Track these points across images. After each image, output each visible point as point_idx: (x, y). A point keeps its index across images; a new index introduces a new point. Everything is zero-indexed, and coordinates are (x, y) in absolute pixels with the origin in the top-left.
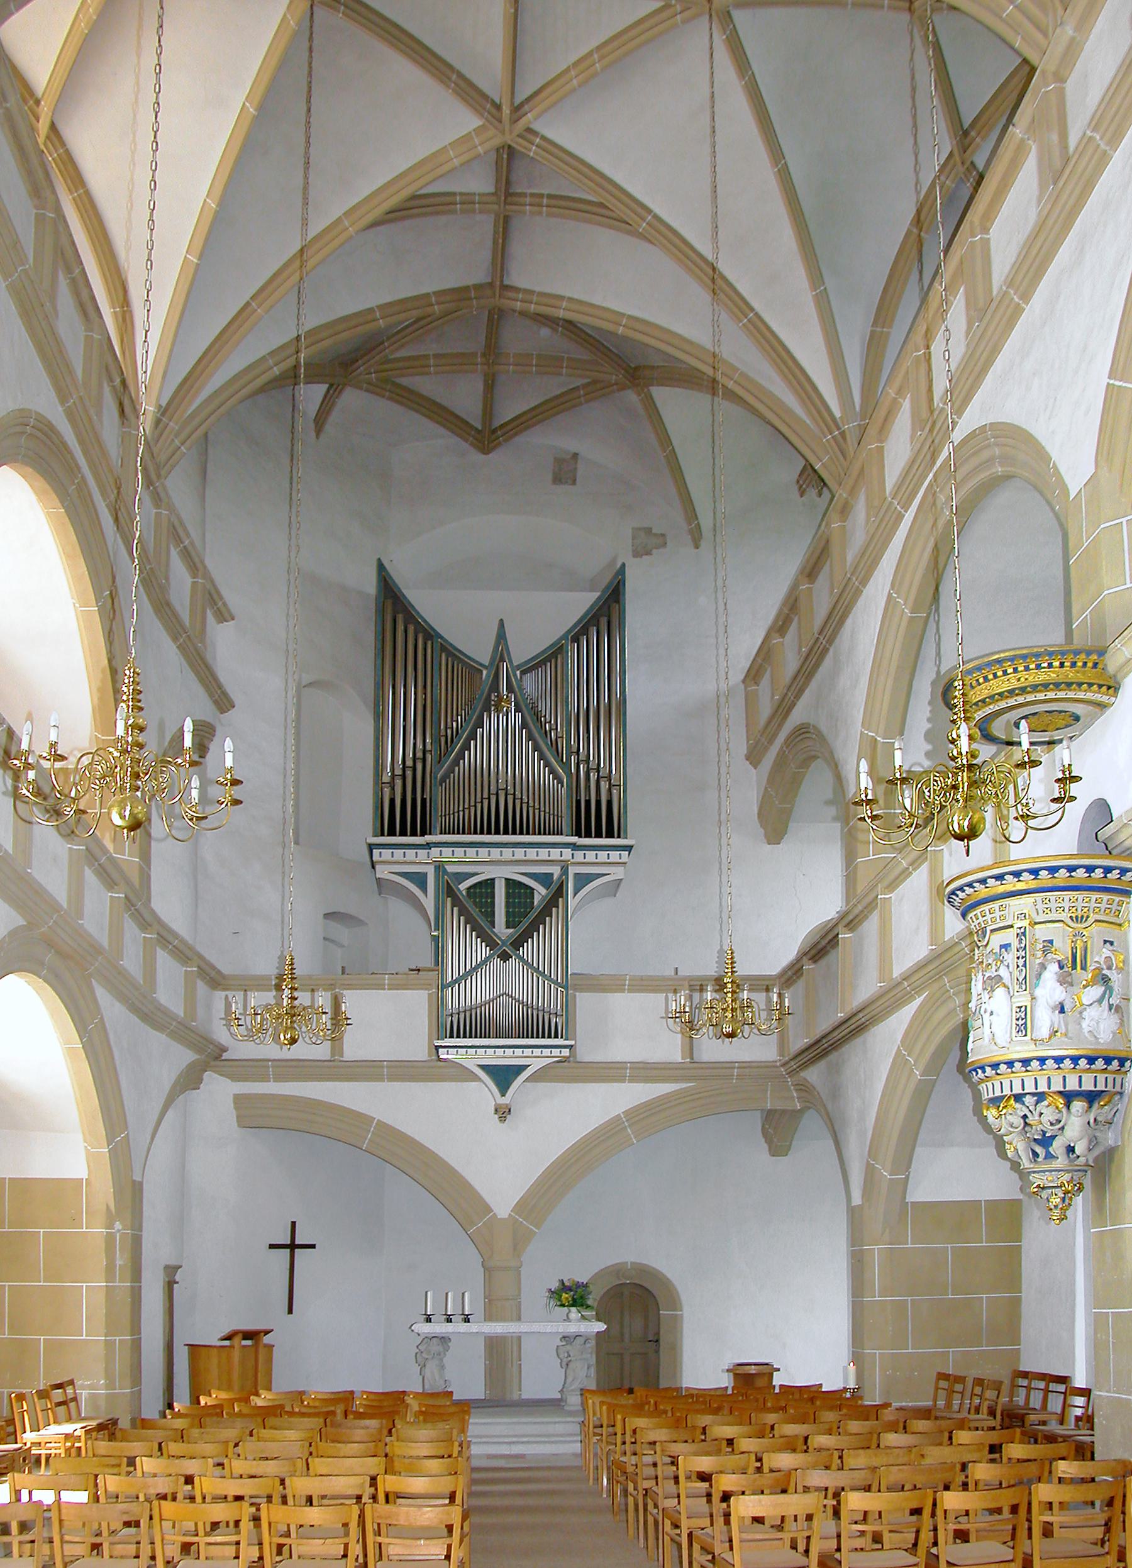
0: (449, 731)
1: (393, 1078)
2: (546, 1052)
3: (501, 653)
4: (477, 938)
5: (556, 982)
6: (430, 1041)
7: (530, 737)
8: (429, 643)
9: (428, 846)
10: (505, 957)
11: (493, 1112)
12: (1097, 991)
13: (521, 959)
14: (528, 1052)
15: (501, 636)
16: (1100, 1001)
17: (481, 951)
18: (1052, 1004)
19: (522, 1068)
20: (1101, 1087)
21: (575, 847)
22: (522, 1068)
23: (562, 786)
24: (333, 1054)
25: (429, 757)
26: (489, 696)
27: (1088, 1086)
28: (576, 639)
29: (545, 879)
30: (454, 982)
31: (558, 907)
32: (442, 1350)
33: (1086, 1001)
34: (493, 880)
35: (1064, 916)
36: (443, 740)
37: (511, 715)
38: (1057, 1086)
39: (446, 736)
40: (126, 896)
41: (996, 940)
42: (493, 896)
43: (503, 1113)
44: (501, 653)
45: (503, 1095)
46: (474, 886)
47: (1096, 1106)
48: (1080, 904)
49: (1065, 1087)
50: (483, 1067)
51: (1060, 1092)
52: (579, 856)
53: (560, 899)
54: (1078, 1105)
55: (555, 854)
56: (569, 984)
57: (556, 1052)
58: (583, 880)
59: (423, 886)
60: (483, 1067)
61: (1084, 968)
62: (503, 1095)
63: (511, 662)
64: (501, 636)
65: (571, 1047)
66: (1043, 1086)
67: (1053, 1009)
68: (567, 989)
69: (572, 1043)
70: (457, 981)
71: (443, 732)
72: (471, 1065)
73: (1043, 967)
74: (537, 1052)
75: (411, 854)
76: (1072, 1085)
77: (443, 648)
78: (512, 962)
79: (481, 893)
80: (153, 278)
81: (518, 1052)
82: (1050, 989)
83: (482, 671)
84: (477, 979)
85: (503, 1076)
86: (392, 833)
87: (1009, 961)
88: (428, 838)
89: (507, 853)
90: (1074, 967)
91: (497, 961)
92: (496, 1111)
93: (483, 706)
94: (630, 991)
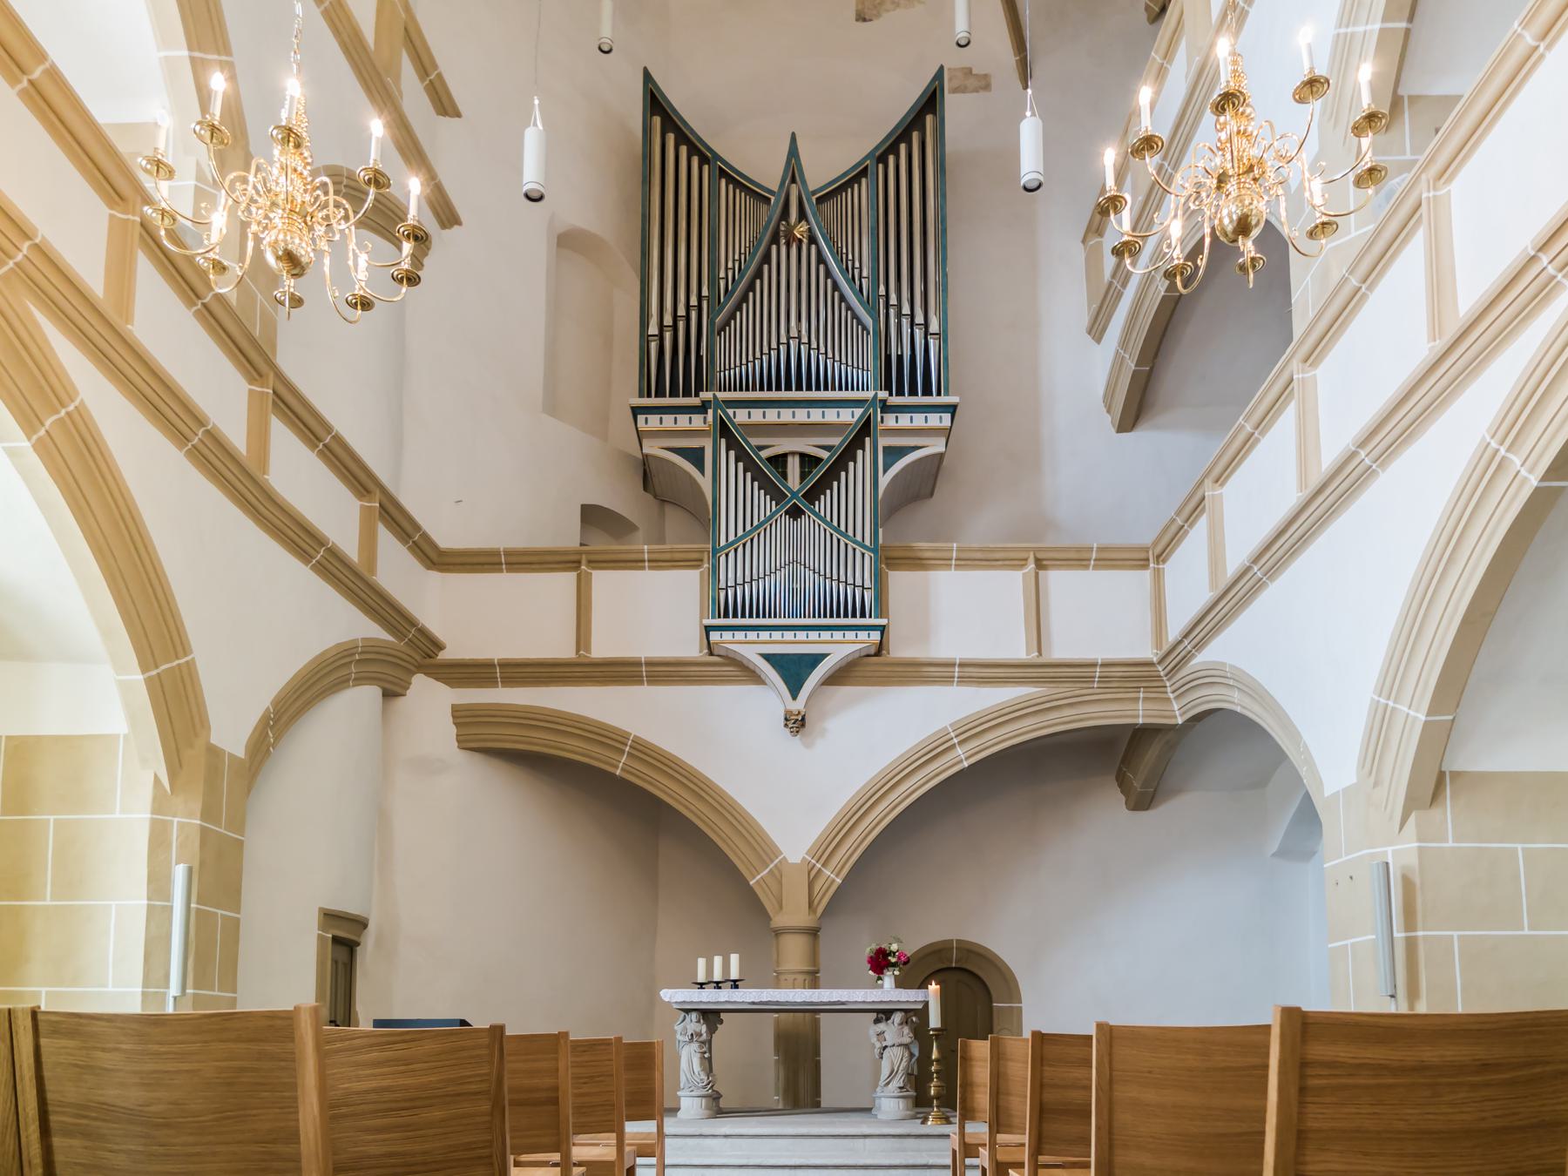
1: (655, 679)
2: (850, 635)
3: (793, 172)
4: (753, 480)
6: (701, 622)
11: (782, 722)
13: (817, 515)
14: (826, 635)
17: (764, 505)
19: (817, 659)
22: (816, 659)
25: (705, 304)
28: (882, 159)
32: (704, 1028)
34: (785, 456)
40: (275, 392)
44: (793, 172)
45: (794, 697)
50: (768, 657)
57: (863, 635)
60: (768, 657)
62: (794, 697)
63: (804, 182)
65: (883, 629)
68: (874, 550)
69: (883, 622)
71: (722, 275)
74: (838, 635)
75: (683, 421)
81: (813, 635)
85: (794, 670)
92: (786, 719)
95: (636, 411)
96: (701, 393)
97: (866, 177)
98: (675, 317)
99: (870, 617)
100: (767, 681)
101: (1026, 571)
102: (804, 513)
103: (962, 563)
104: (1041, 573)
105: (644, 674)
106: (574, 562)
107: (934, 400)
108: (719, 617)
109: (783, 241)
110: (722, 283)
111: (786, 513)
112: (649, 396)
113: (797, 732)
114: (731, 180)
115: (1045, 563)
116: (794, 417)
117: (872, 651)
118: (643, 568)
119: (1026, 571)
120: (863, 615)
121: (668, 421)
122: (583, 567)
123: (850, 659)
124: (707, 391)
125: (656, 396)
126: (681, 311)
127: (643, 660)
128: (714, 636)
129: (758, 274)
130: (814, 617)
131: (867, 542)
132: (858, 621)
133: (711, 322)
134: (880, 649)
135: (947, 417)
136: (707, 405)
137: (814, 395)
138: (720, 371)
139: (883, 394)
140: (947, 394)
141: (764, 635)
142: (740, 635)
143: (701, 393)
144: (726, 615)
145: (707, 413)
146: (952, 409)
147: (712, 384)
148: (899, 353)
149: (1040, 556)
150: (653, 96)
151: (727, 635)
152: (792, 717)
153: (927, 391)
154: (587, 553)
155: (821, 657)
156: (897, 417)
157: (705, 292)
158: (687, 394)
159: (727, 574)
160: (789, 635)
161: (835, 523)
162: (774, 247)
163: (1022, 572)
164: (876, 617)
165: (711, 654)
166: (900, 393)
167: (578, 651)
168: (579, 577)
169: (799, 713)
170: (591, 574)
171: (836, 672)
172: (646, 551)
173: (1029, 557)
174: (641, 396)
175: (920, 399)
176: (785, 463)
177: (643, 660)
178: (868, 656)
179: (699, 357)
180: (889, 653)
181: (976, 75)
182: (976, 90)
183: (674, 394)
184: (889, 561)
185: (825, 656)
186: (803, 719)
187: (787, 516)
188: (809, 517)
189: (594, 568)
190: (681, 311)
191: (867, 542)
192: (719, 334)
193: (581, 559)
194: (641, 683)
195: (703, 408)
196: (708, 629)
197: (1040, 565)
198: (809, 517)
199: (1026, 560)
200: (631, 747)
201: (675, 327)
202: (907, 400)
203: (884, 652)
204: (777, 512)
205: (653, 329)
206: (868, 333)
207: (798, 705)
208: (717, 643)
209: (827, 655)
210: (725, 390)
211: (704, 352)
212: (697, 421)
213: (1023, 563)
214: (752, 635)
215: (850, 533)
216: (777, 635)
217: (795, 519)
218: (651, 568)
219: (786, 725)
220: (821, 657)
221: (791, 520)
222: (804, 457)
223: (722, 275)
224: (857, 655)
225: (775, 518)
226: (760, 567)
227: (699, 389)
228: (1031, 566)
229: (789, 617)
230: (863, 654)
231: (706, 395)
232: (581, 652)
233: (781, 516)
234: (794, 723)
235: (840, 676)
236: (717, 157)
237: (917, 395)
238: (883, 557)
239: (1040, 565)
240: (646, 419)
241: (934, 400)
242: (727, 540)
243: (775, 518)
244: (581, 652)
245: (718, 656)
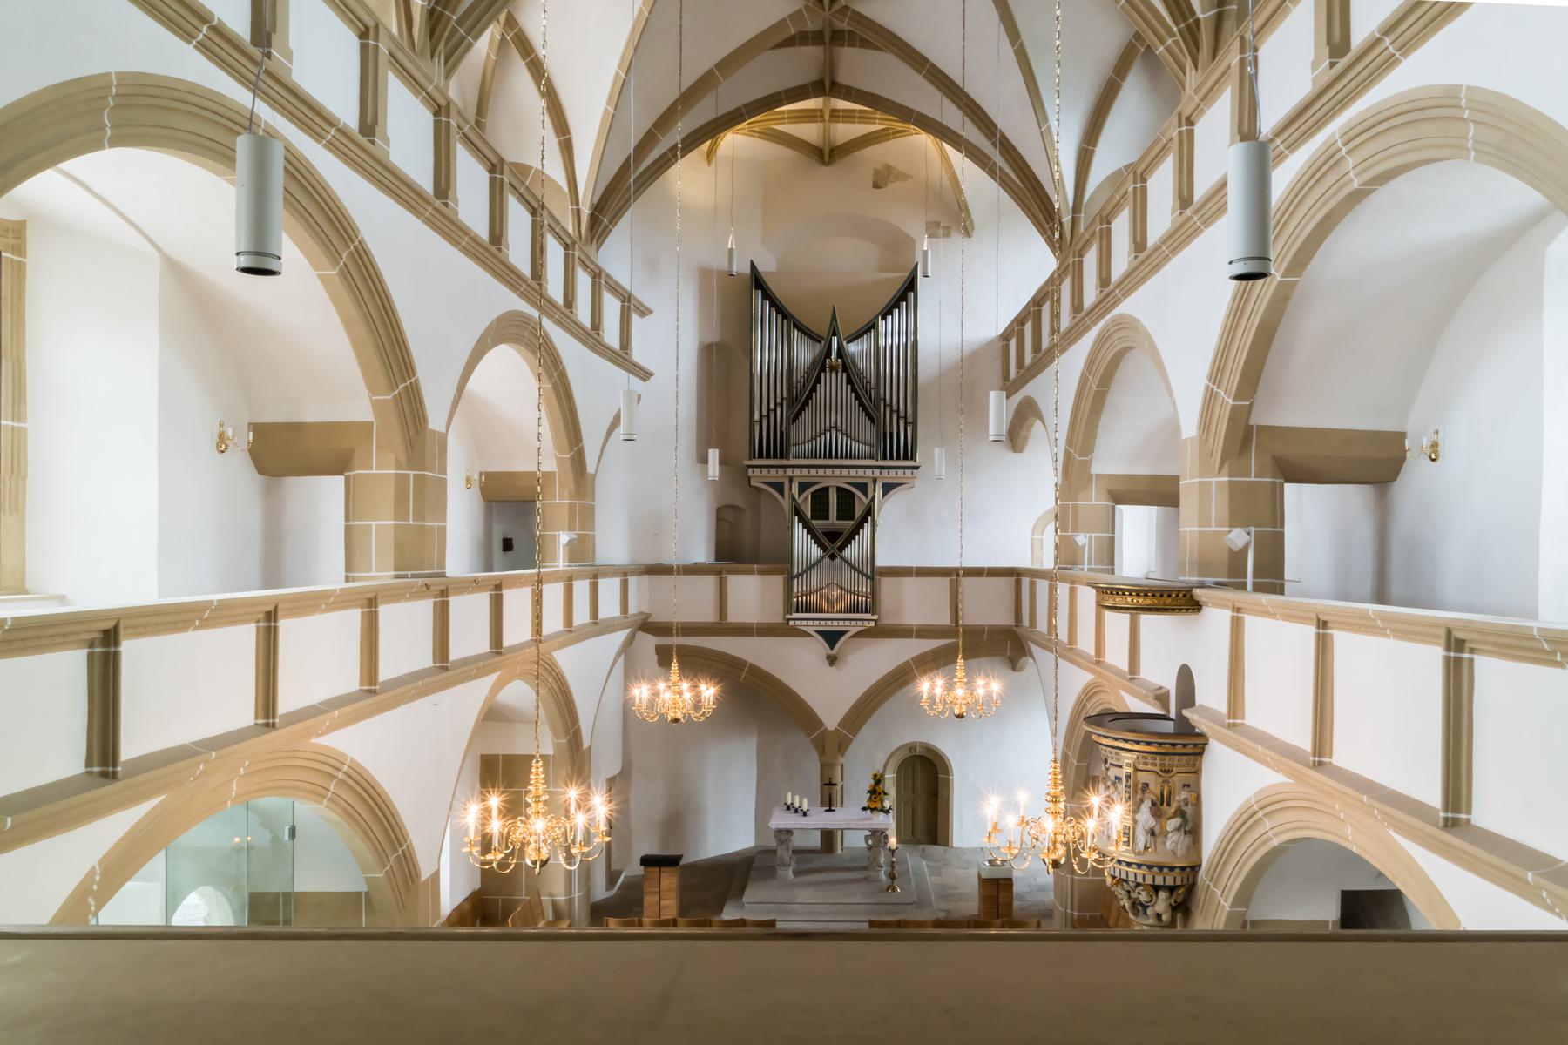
0: (799, 385)
2: (860, 623)
5: (867, 577)
7: (854, 390)
8: (785, 321)
10: (833, 557)
12: (1176, 822)
14: (847, 623)
15: (834, 318)
16: (1178, 829)
18: (1147, 828)
19: (843, 633)
20: (1179, 882)
24: (721, 618)
27: (1170, 882)
28: (884, 318)
29: (863, 488)
33: (1169, 829)
35: (1157, 769)
38: (1149, 881)
39: (797, 388)
41: (1113, 772)
42: (827, 497)
43: (832, 660)
46: (817, 491)
47: (1175, 893)
48: (1167, 762)
49: (1154, 882)
50: (818, 632)
51: (1151, 885)
52: (885, 472)
54: (1162, 895)
55: (869, 472)
56: (875, 574)
57: (866, 623)
58: (888, 488)
59: (782, 493)
60: (818, 632)
61: (1169, 804)
62: (832, 648)
64: (834, 318)
65: (875, 621)
66: (1140, 880)
67: (1147, 832)
69: (875, 617)
71: (794, 386)
72: (810, 630)
73: (1142, 801)
74: (854, 623)
76: (1159, 881)
78: (838, 560)
80: (448, 811)
82: (1145, 817)
84: (814, 572)
85: (831, 638)
86: (761, 456)
87: (1120, 790)
88: (785, 462)
90: (1162, 804)
91: (827, 560)
93: (820, 369)
97: (874, 328)
98: (769, 410)
110: (795, 390)
114: (799, 329)
129: (814, 389)
131: (869, 573)
133: (788, 418)
141: (817, 623)
142: (804, 623)
146: (917, 468)
150: (756, 276)
159: (798, 586)
162: (823, 374)
163: (949, 579)
174: (750, 459)
179: (781, 433)
190: (772, 406)
191: (869, 573)
201: (768, 416)
205: (757, 417)
211: (784, 429)
214: (810, 623)
223: (794, 386)
226: (815, 586)
235: (853, 636)
236: (793, 317)
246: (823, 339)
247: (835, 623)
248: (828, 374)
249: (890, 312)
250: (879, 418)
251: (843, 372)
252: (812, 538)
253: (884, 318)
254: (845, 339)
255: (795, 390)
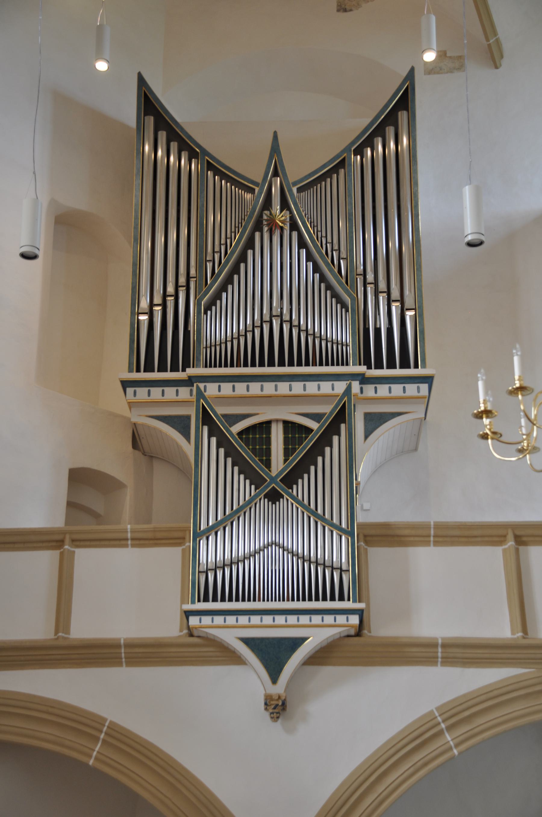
0: (217, 256)
2: (329, 619)
9: (190, 382)
11: (263, 706)
13: (295, 499)
14: (304, 619)
19: (297, 642)
21: (364, 380)
22: (297, 642)
23: (347, 311)
26: (261, 216)
30: (209, 529)
31: (339, 435)
36: (209, 265)
37: (286, 233)
45: (274, 680)
50: (248, 642)
53: (343, 426)
57: (341, 619)
60: (248, 642)
62: (274, 680)
65: (360, 613)
69: (361, 606)
70: (213, 529)
74: (316, 619)
77: (210, 166)
79: (254, 439)
81: (292, 619)
83: (254, 190)
89: (283, 388)
92: (266, 704)
94: (436, 544)
95: (126, 384)
96: (187, 369)
98: (165, 295)
99: (349, 600)
100: (247, 662)
101: (506, 546)
102: (282, 497)
103: (440, 539)
104: (521, 548)
105: (123, 655)
106: (57, 541)
107: (411, 372)
108: (199, 601)
109: (266, 229)
111: (265, 497)
112: (138, 370)
113: (278, 718)
115: (524, 539)
116: (276, 390)
117: (352, 632)
118: (126, 546)
119: (506, 546)
120: (341, 598)
121: (156, 392)
122: (66, 547)
123: (329, 641)
124: (193, 367)
125: (145, 371)
126: (171, 289)
127: (122, 642)
128: (194, 621)
130: (293, 600)
131: (344, 525)
132: (337, 605)
134: (359, 631)
135: (424, 387)
136: (193, 380)
137: (296, 370)
138: (206, 347)
139: (362, 369)
140: (424, 366)
141: (243, 620)
142: (219, 620)
143: (187, 369)
144: (206, 599)
145: (193, 386)
146: (428, 380)
147: (198, 360)
148: (378, 326)
149: (518, 533)
151: (207, 620)
152: (272, 702)
153: (405, 364)
154: (71, 533)
155: (301, 641)
156: (376, 388)
157: (193, 272)
158: (174, 369)
160: (268, 620)
161: (313, 506)
164: (354, 601)
165: (191, 635)
166: (379, 365)
167: (57, 632)
168: (62, 554)
169: (279, 697)
170: (74, 552)
171: (317, 652)
172: (129, 530)
173: (507, 534)
174: (130, 370)
175: (398, 372)
176: (269, 432)
177: (122, 642)
178: (348, 636)
180: (370, 632)
181: (450, 57)
182: (451, 71)
183: (162, 368)
184: (368, 538)
185: (304, 639)
186: (284, 704)
187: (266, 500)
188: (287, 500)
189: (78, 547)
190: (171, 289)
191: (344, 525)
192: (206, 313)
193: (65, 538)
194: (120, 664)
195: (190, 382)
196: (188, 614)
197: (520, 541)
198: (287, 500)
199: (505, 536)
200: (106, 734)
202: (385, 372)
203: (365, 632)
204: (256, 496)
205: (144, 304)
206: (347, 311)
207: (279, 688)
208: (196, 628)
209: (306, 639)
210: (210, 366)
212: (184, 393)
213: (502, 539)
214: (231, 620)
215: (327, 516)
216: (255, 620)
217: (274, 503)
218: (133, 546)
219: (266, 709)
220: (301, 641)
221: (270, 503)
222: (289, 426)
224: (338, 636)
225: (255, 502)
227: (186, 364)
228: (511, 543)
229: (268, 600)
230: (343, 635)
231: (191, 371)
232: (60, 634)
233: (260, 500)
234: (274, 708)
237: (396, 368)
238: (361, 536)
239: (520, 541)
240: (135, 392)
241: (411, 372)
242: (208, 525)
243: (255, 502)
244: (60, 634)
245: (199, 637)
246: (257, 184)
247: (280, 619)
248: (266, 236)
249: (369, 142)
250: (355, 300)
251: (291, 230)
252: (240, 473)
253: (359, 151)
254: (294, 184)
255: (209, 265)
